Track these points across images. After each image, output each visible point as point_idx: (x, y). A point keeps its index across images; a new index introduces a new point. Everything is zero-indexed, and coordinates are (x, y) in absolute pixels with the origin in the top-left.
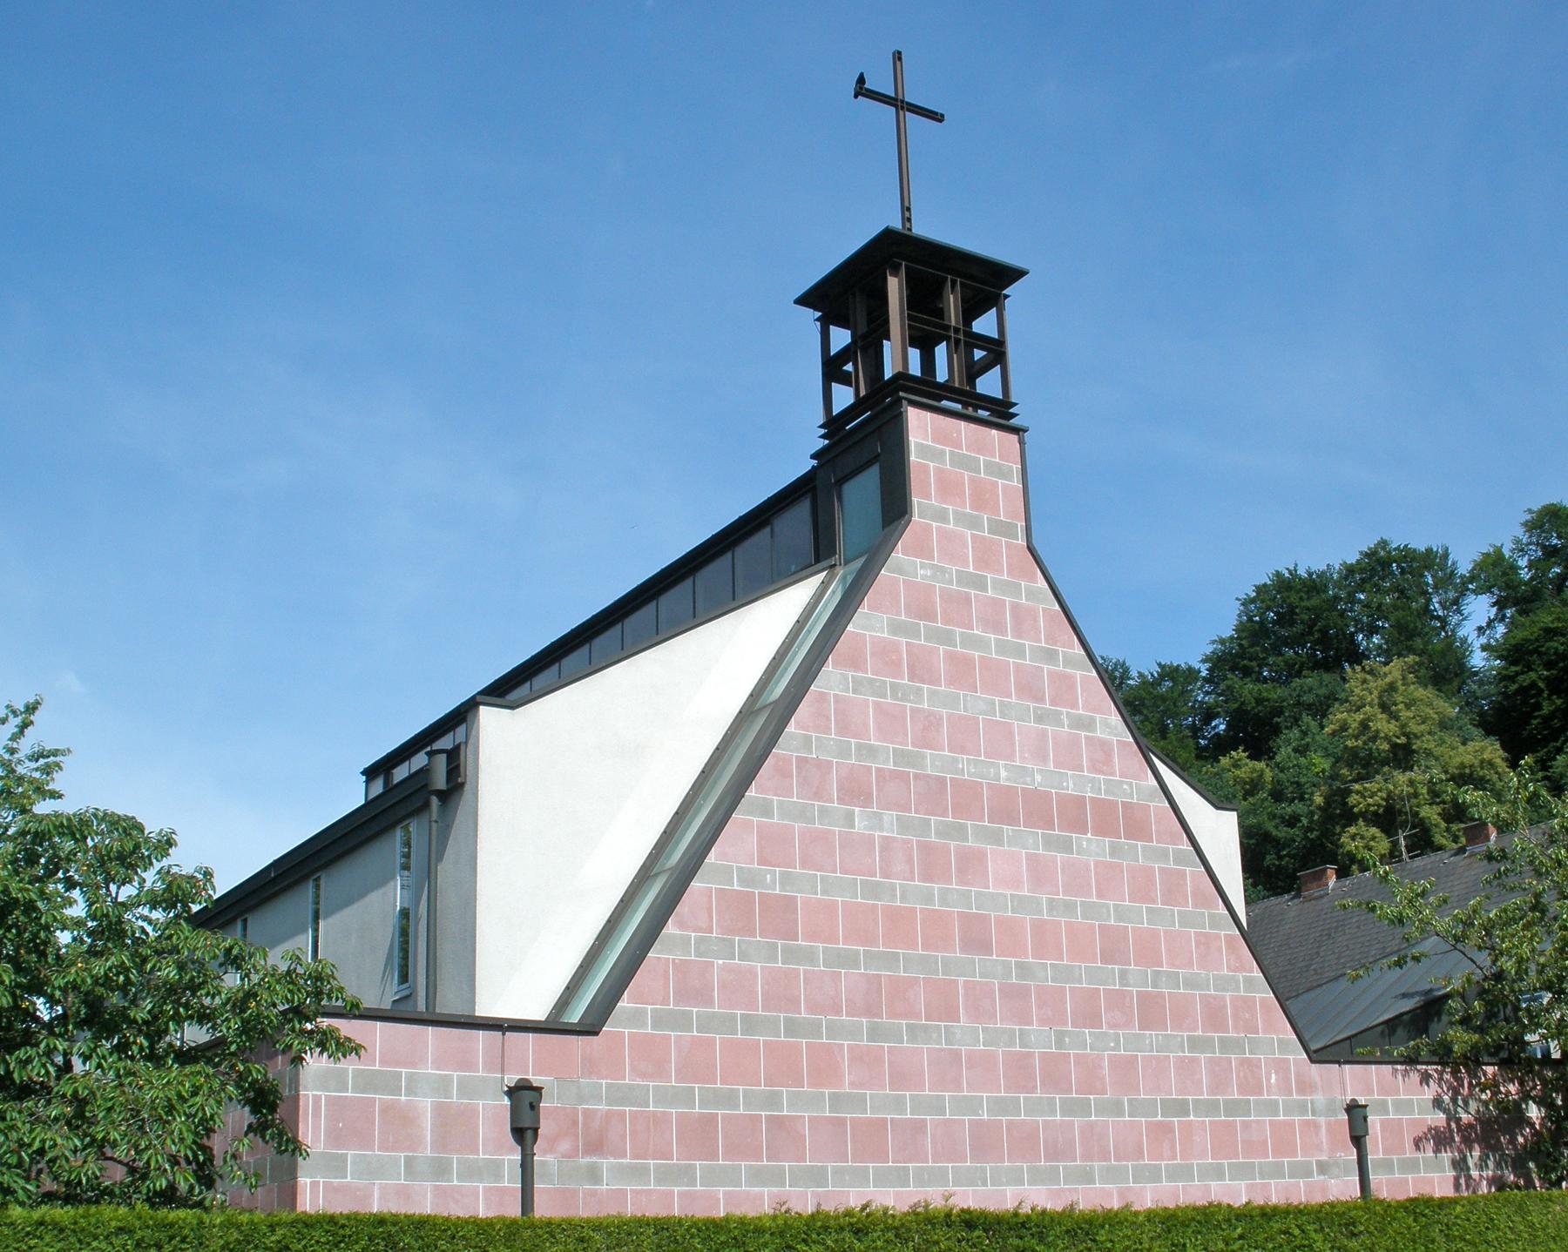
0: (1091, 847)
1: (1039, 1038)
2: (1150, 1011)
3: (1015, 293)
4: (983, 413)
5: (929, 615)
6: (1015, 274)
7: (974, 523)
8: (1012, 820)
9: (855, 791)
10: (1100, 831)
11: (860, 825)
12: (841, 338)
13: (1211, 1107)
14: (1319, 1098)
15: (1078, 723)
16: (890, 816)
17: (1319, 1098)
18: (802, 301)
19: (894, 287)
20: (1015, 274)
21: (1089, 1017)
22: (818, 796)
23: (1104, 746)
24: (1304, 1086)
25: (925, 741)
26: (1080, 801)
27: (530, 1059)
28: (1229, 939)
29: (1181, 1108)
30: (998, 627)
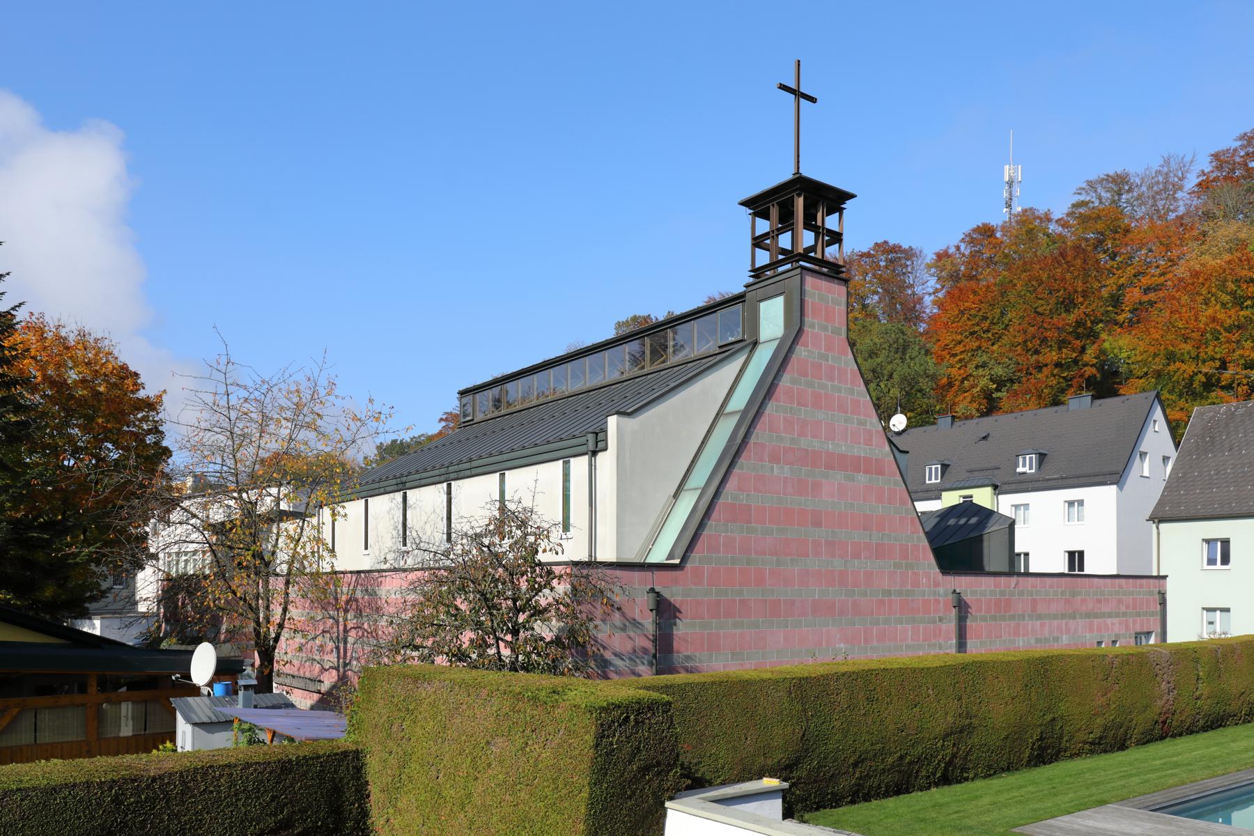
0: (862, 478)
1: (838, 564)
2: (880, 552)
3: (849, 205)
4: (825, 270)
5: (806, 375)
6: (852, 196)
7: (826, 329)
8: (833, 468)
9: (775, 459)
10: (866, 472)
11: (776, 472)
12: (763, 226)
13: (900, 593)
14: (941, 590)
15: (861, 423)
16: (787, 468)
17: (941, 590)
18: (746, 203)
19: (800, 202)
20: (852, 196)
21: (857, 555)
22: (761, 460)
23: (870, 432)
24: (937, 585)
25: (802, 434)
26: (859, 457)
27: (661, 582)
28: (912, 519)
29: (889, 593)
30: (832, 380)
